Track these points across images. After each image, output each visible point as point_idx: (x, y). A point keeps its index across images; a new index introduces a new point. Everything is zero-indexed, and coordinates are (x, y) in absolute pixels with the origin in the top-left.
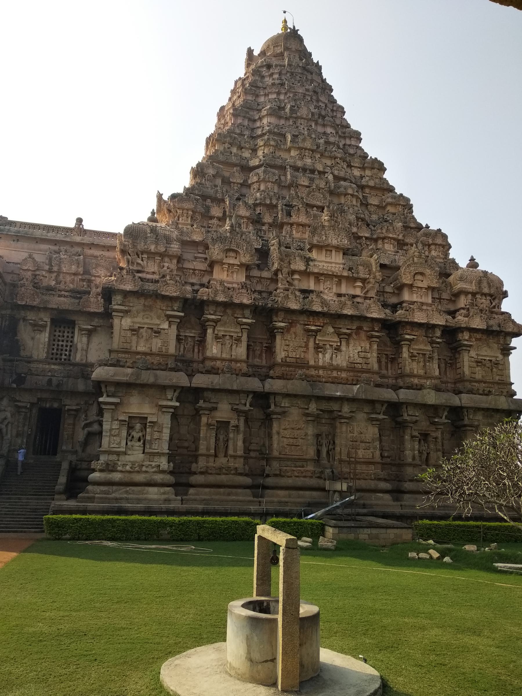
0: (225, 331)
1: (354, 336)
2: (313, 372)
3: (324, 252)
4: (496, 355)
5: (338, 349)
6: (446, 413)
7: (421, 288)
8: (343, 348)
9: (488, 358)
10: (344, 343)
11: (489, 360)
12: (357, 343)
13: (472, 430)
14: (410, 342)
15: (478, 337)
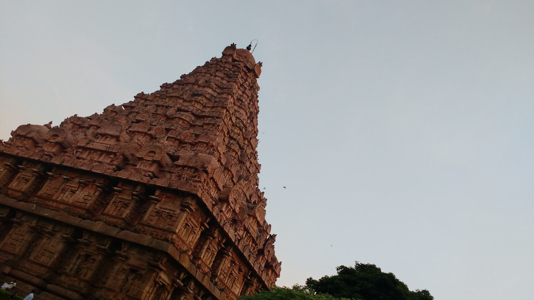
0: (25, 175)
1: (90, 186)
2: (50, 203)
3: (105, 137)
4: (175, 210)
5: (73, 192)
6: (109, 243)
7: (149, 161)
8: (77, 192)
9: (168, 211)
10: (79, 189)
11: (168, 213)
12: (88, 190)
13: (121, 260)
14: (120, 193)
15: (168, 195)
